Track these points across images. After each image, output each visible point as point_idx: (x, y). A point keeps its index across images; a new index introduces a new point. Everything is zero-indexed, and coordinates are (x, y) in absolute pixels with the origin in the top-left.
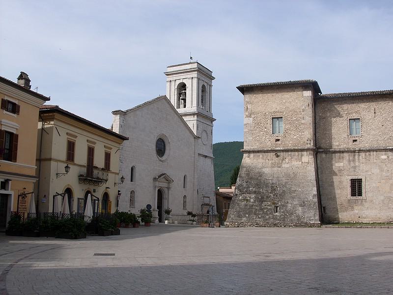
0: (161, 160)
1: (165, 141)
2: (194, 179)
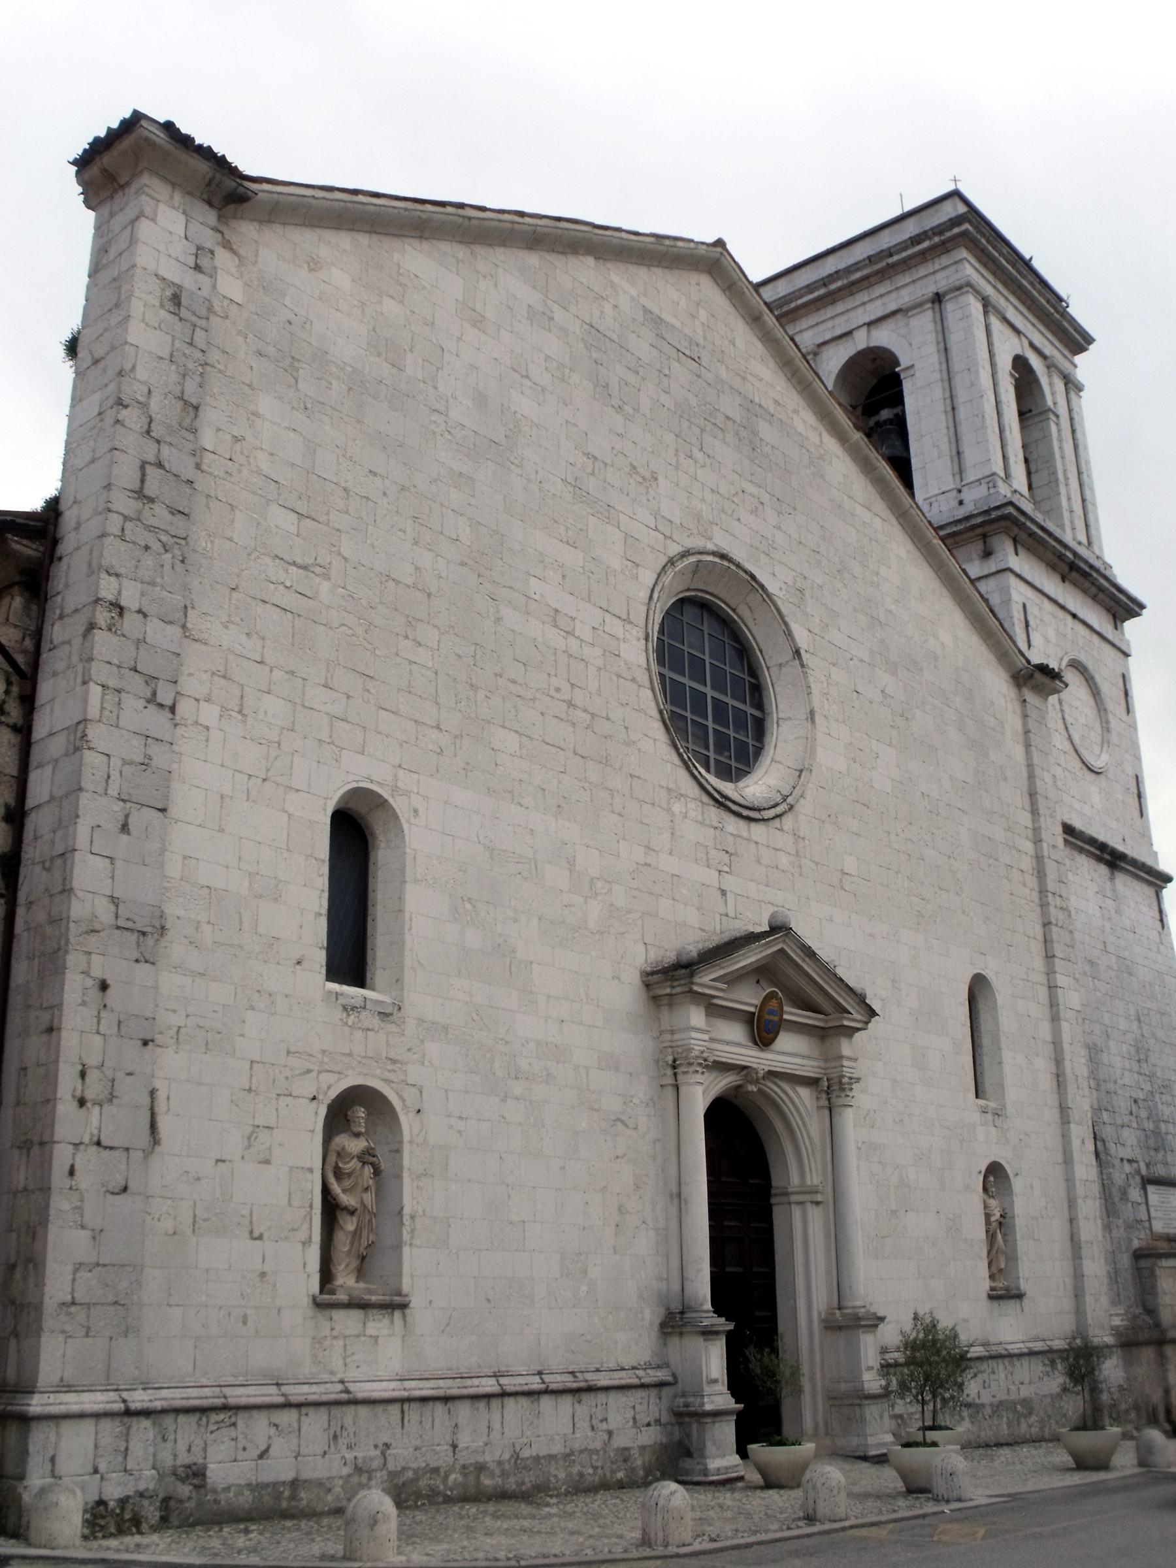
0: (722, 802)
1: (759, 633)
2: (1055, 1018)
